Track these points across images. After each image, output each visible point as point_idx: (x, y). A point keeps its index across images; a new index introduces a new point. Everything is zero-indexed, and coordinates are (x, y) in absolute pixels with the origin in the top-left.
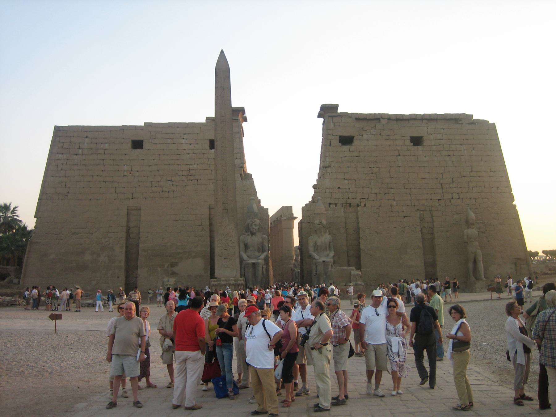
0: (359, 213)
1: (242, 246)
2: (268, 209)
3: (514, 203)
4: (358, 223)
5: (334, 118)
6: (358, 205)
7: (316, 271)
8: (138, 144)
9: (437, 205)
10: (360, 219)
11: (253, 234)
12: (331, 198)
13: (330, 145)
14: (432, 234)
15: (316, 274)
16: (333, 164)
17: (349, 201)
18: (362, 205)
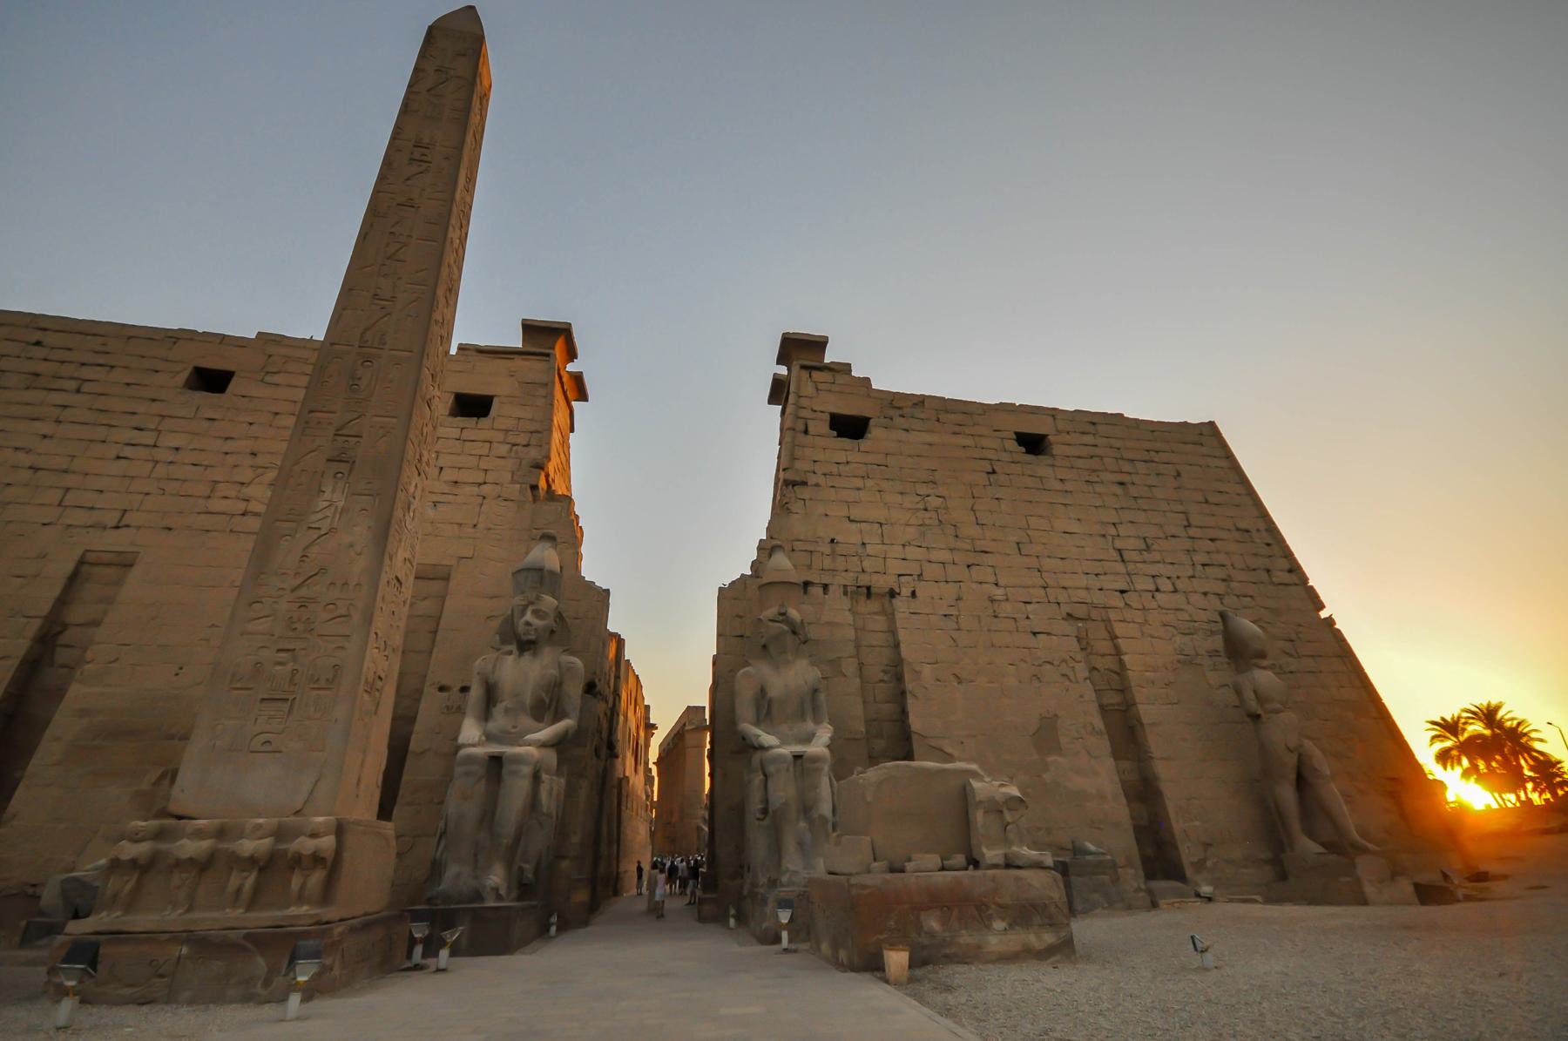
0: (898, 616)
1: (476, 692)
2: (607, 591)
3: (1323, 614)
4: (897, 646)
5: (816, 375)
6: (893, 594)
7: (766, 801)
8: (212, 381)
9: (1121, 604)
10: (902, 635)
11: (526, 646)
12: (810, 567)
13: (806, 432)
14: (1124, 690)
15: (765, 811)
16: (812, 480)
17: (864, 580)
18: (906, 592)
